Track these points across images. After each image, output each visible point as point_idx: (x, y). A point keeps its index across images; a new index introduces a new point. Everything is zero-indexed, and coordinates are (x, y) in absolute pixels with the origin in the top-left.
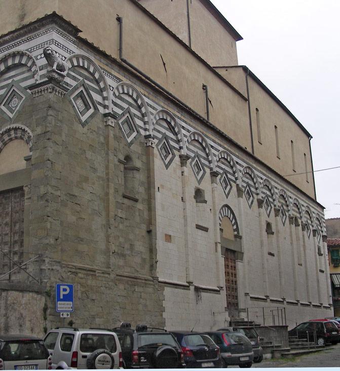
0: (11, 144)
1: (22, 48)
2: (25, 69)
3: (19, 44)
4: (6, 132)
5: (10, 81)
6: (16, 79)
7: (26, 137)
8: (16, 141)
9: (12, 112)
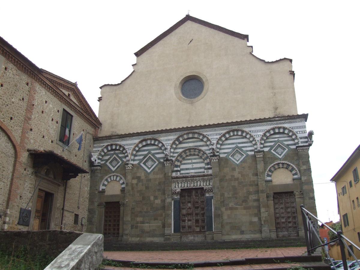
0: (279, 170)
1: (286, 125)
2: (285, 135)
3: (284, 123)
4: (277, 164)
5: (276, 139)
6: (280, 139)
7: (290, 168)
8: (282, 169)
9: (280, 155)
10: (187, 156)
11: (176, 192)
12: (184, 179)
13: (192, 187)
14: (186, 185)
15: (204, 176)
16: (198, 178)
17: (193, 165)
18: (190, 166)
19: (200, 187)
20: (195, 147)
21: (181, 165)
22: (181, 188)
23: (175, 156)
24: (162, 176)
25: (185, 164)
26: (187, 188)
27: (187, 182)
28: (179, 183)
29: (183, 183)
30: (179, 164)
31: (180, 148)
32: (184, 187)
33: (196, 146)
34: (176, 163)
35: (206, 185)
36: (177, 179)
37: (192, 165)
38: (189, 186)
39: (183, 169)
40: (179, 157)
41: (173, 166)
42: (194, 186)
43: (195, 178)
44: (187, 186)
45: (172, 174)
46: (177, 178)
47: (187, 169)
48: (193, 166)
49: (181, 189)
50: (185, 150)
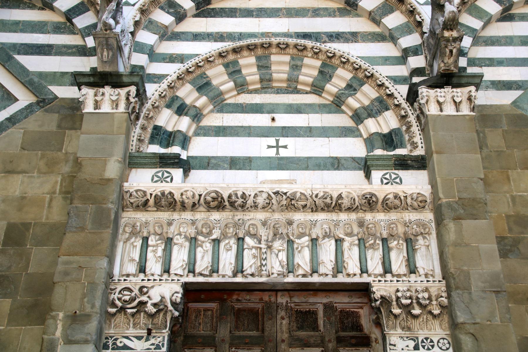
10: (241, 87)
11: (143, 304)
12: (216, 216)
13: (274, 278)
14: (227, 260)
15: (370, 203)
16: (321, 216)
17: (283, 141)
18: (259, 147)
19: (341, 279)
20: (303, 42)
21: (197, 134)
22: (191, 279)
23: (164, 76)
24: (47, 187)
25: (221, 131)
26: (239, 279)
27: (240, 240)
28: (178, 240)
29: (208, 246)
30: (184, 124)
31: (197, 37)
32: (214, 270)
33: (306, 36)
34: (167, 119)
35: (387, 270)
36: (164, 216)
37: (272, 141)
38: (249, 263)
39: (207, 163)
40: (188, 87)
41: (138, 130)
42: (291, 268)
43: (298, 217)
44: (239, 270)
45: (124, 178)
46: (167, 202)
47: (235, 163)
48: (277, 147)
49: (188, 288)
50: (235, 51)
